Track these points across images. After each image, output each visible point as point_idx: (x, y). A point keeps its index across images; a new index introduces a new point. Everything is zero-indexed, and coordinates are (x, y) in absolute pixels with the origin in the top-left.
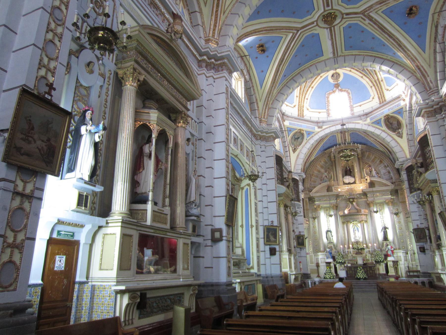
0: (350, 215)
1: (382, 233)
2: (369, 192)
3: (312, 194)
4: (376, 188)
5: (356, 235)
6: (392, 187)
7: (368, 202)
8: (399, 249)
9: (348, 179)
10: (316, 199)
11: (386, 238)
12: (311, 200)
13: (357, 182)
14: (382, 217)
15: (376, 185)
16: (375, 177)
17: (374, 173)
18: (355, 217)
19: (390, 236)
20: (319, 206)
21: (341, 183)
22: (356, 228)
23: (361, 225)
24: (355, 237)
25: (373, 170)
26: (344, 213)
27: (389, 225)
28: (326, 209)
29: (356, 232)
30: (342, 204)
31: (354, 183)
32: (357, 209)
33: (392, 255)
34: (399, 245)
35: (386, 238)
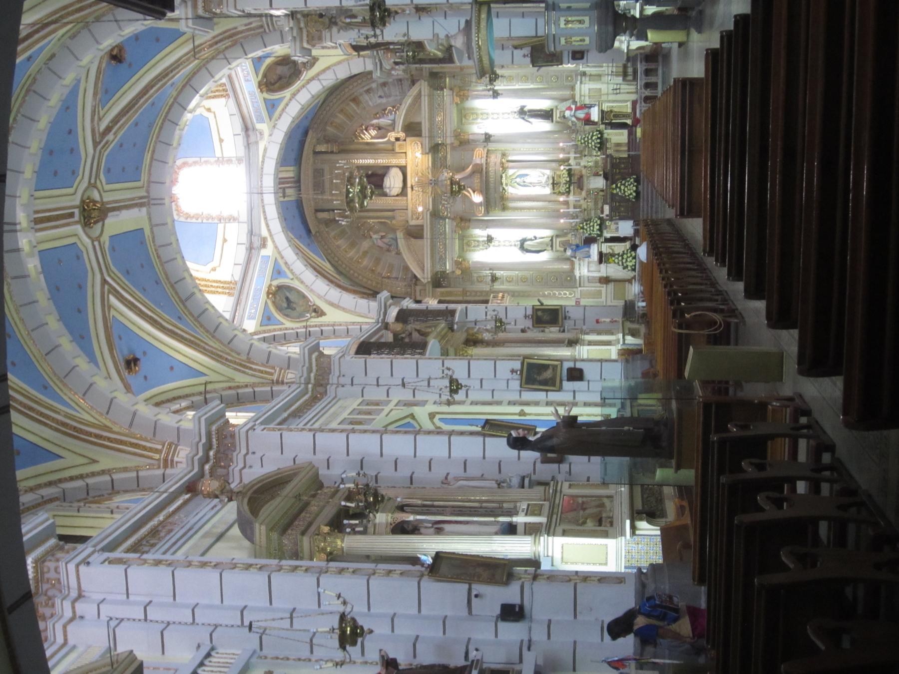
0: (485, 190)
1: (531, 120)
2: (431, 137)
3: (425, 277)
4: (424, 118)
5: (535, 180)
6: (423, 86)
7: (457, 143)
8: (573, 88)
9: (393, 182)
10: (438, 268)
11: (547, 115)
12: (439, 280)
13: (402, 162)
14: (495, 116)
15: (417, 120)
16: (394, 121)
17: (383, 121)
18: (492, 180)
19: (544, 104)
20: (458, 264)
21: (401, 202)
22: (518, 180)
23: (513, 168)
24: (540, 183)
25: (375, 121)
26: (480, 204)
27: (516, 103)
28: (466, 244)
29: (528, 180)
30: (458, 206)
31: (403, 169)
32: (473, 172)
33: (586, 111)
34: (566, 88)
35: (547, 115)
